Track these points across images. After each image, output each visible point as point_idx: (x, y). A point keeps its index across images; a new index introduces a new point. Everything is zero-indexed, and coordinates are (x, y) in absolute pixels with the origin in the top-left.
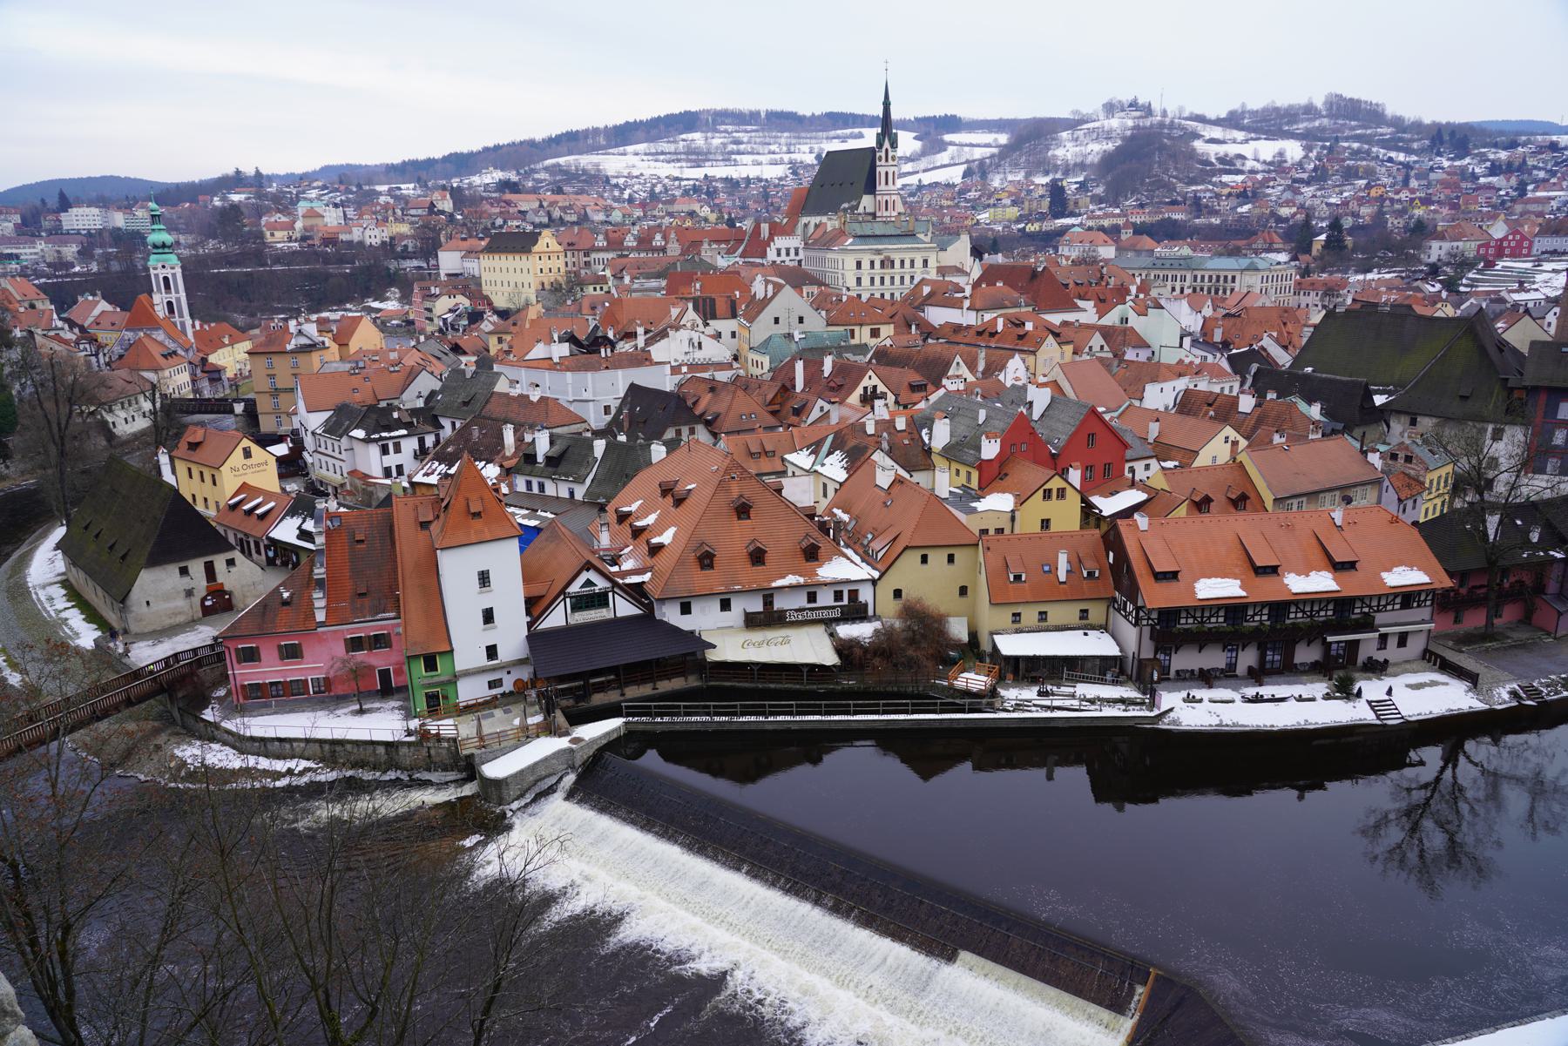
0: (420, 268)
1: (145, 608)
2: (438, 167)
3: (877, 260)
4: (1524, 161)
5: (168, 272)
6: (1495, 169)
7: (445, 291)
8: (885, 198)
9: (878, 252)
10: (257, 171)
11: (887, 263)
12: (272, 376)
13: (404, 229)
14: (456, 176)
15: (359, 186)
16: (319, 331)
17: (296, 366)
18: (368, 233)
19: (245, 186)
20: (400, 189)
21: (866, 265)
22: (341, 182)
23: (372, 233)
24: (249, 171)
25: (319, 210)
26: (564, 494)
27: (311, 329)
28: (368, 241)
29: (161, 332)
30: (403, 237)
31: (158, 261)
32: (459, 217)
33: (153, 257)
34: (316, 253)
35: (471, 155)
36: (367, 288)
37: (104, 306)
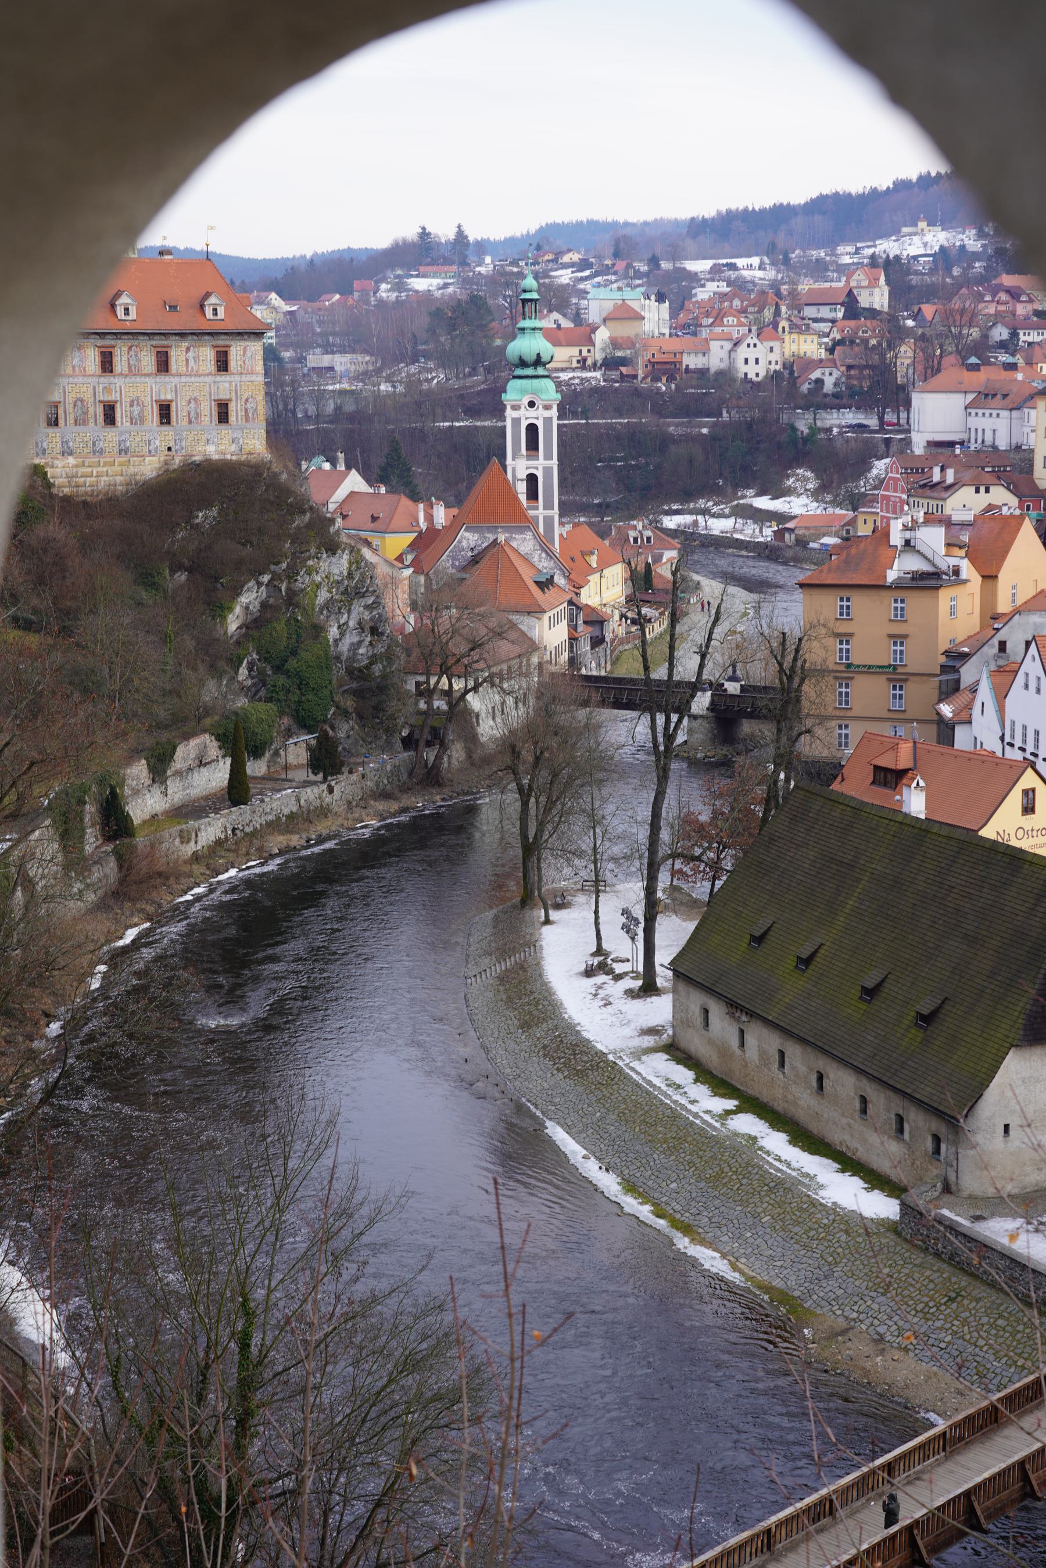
0: (862, 427)
1: (998, 1139)
2: (798, 223)
5: (537, 416)
7: (967, 475)
10: (461, 235)
12: (845, 638)
13: (810, 347)
14: (844, 240)
15: (654, 262)
16: (948, 545)
17: (901, 617)
18: (743, 352)
19: (434, 263)
20: (733, 267)
22: (616, 255)
23: (752, 354)
24: (444, 232)
25: (635, 306)
27: (933, 538)
28: (742, 369)
29: (529, 535)
30: (810, 364)
31: (523, 392)
32: (910, 323)
33: (513, 385)
34: (637, 393)
35: (874, 195)
36: (745, 468)
37: (354, 482)
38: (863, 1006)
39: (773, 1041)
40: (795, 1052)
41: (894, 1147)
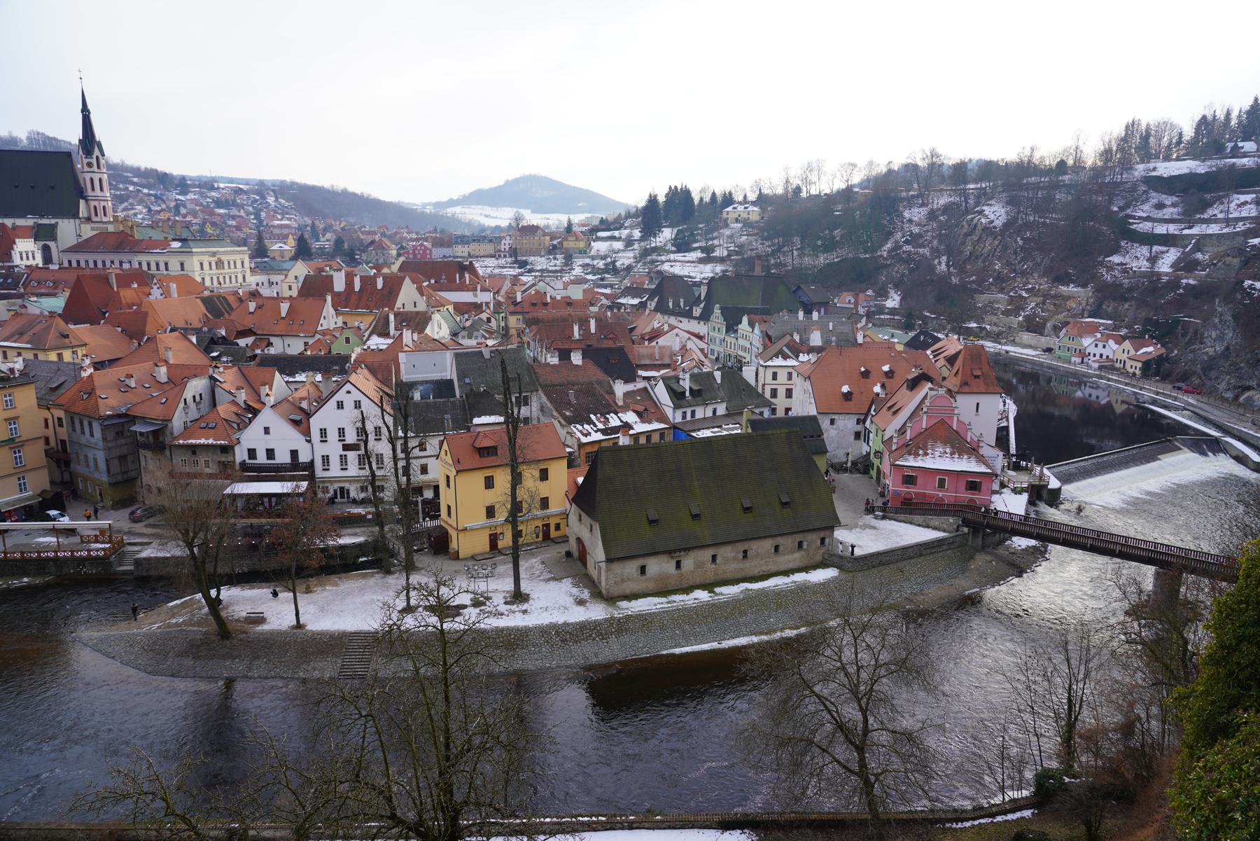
3: (214, 260)
4: (234, 201)
6: (219, 203)
8: (103, 204)
9: (214, 254)
11: (220, 264)
21: (206, 266)
26: (709, 413)
38: (750, 515)
39: (707, 554)
40: (726, 552)
41: (797, 555)
